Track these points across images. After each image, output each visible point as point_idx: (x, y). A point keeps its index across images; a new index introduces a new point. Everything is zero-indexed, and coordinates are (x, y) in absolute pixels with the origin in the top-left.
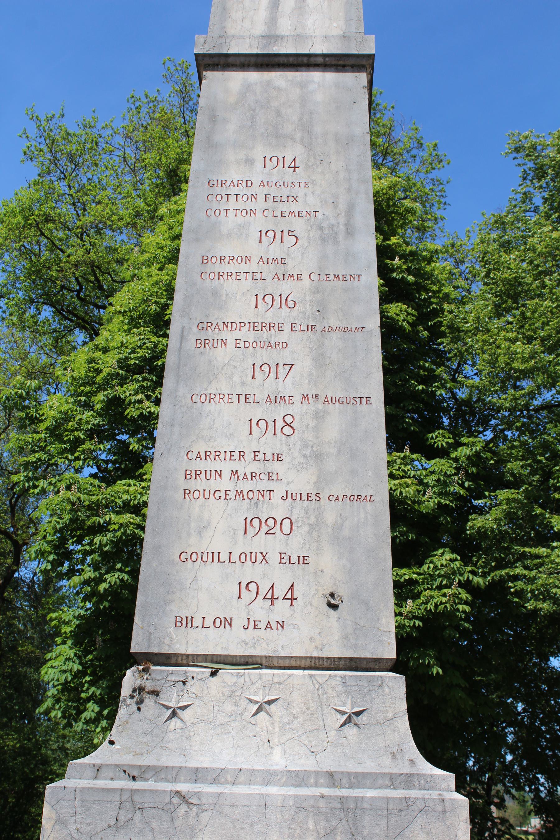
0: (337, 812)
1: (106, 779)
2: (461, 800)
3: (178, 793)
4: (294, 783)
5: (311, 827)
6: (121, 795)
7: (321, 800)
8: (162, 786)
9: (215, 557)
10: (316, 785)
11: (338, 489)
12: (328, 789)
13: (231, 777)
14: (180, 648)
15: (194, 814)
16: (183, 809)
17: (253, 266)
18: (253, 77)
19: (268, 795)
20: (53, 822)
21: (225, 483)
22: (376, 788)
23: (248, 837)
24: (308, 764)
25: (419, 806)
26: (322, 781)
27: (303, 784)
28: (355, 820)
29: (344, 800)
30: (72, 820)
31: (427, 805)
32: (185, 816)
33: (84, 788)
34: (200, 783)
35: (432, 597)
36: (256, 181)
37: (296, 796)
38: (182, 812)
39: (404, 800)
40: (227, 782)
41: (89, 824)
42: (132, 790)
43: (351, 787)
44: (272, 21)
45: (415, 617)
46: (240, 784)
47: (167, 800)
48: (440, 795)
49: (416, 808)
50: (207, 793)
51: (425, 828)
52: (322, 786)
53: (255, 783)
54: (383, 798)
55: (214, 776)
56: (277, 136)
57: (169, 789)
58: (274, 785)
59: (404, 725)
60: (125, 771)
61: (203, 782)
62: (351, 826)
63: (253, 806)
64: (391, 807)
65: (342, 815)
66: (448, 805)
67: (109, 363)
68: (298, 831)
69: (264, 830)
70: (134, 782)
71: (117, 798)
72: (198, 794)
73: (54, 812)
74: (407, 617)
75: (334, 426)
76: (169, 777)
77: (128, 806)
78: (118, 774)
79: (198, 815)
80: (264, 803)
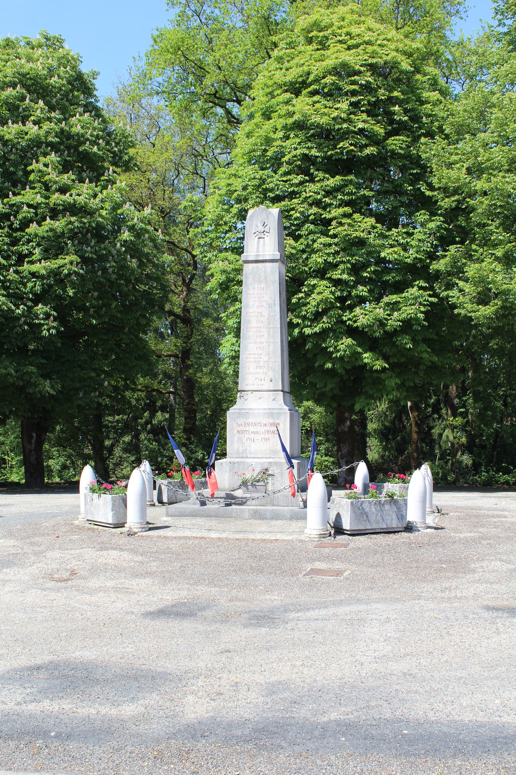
9: (251, 373)
11: (272, 360)
14: (246, 389)
17: (256, 314)
18: (254, 265)
21: (253, 360)
24: (267, 407)
35: (406, 310)
36: (256, 293)
44: (258, 249)
45: (399, 321)
59: (282, 400)
67: (238, 184)
74: (394, 321)
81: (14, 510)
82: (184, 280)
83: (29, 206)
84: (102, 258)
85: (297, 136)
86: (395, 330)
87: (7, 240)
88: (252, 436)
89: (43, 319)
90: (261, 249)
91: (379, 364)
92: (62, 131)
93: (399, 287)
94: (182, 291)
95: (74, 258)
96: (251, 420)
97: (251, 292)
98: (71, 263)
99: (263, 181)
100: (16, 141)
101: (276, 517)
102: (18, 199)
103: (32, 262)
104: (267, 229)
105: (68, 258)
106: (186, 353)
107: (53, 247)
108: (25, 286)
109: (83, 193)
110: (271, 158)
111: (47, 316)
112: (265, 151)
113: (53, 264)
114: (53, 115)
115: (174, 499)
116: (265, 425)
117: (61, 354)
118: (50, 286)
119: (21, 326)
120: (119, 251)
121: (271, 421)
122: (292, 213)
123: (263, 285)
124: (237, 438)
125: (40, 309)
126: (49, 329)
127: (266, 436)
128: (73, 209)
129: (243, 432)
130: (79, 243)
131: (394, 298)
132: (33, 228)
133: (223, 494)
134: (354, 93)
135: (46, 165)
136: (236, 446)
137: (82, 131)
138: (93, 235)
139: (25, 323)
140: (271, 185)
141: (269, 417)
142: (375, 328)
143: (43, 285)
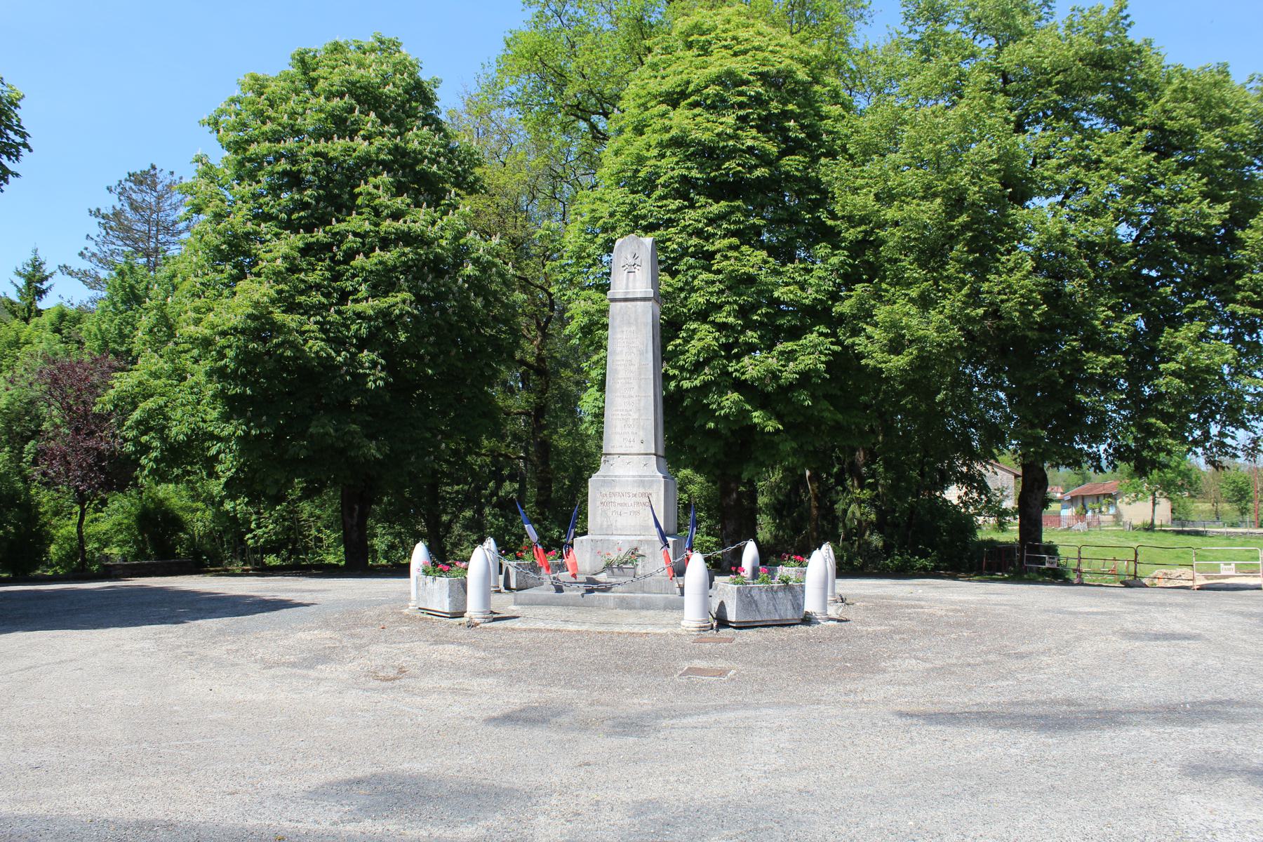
44: (627, 287)
56: (629, 324)
67: (604, 210)
75: (642, 404)
81: (331, 596)
82: (538, 324)
83: (356, 234)
84: (440, 297)
85: (674, 154)
86: (791, 383)
87: (328, 274)
88: (619, 509)
89: (369, 368)
90: (631, 285)
91: (1145, 271)
92: (396, 147)
93: (795, 334)
94: (536, 336)
95: (407, 295)
96: (617, 490)
97: (619, 336)
98: (404, 302)
99: (634, 207)
100: (342, 158)
101: (647, 606)
102: (342, 226)
103: (357, 301)
104: (638, 262)
105: (401, 296)
106: (538, 412)
107: (383, 282)
108: (348, 329)
109: (419, 219)
110: (644, 179)
111: (374, 364)
112: (637, 171)
113: (382, 303)
114: (386, 128)
115: (523, 585)
117: (393, 410)
118: (378, 329)
119: (342, 376)
120: (460, 288)
121: (642, 490)
122: (668, 244)
123: (633, 328)
125: (366, 356)
126: (376, 380)
127: (636, 508)
128: (407, 238)
130: (414, 278)
131: (790, 346)
132: (359, 260)
133: (581, 578)
134: (741, 106)
135: (377, 187)
136: (599, 520)
137: (419, 148)
138: (430, 268)
139: (347, 372)
140: (644, 212)
142: (767, 381)
143: (369, 327)
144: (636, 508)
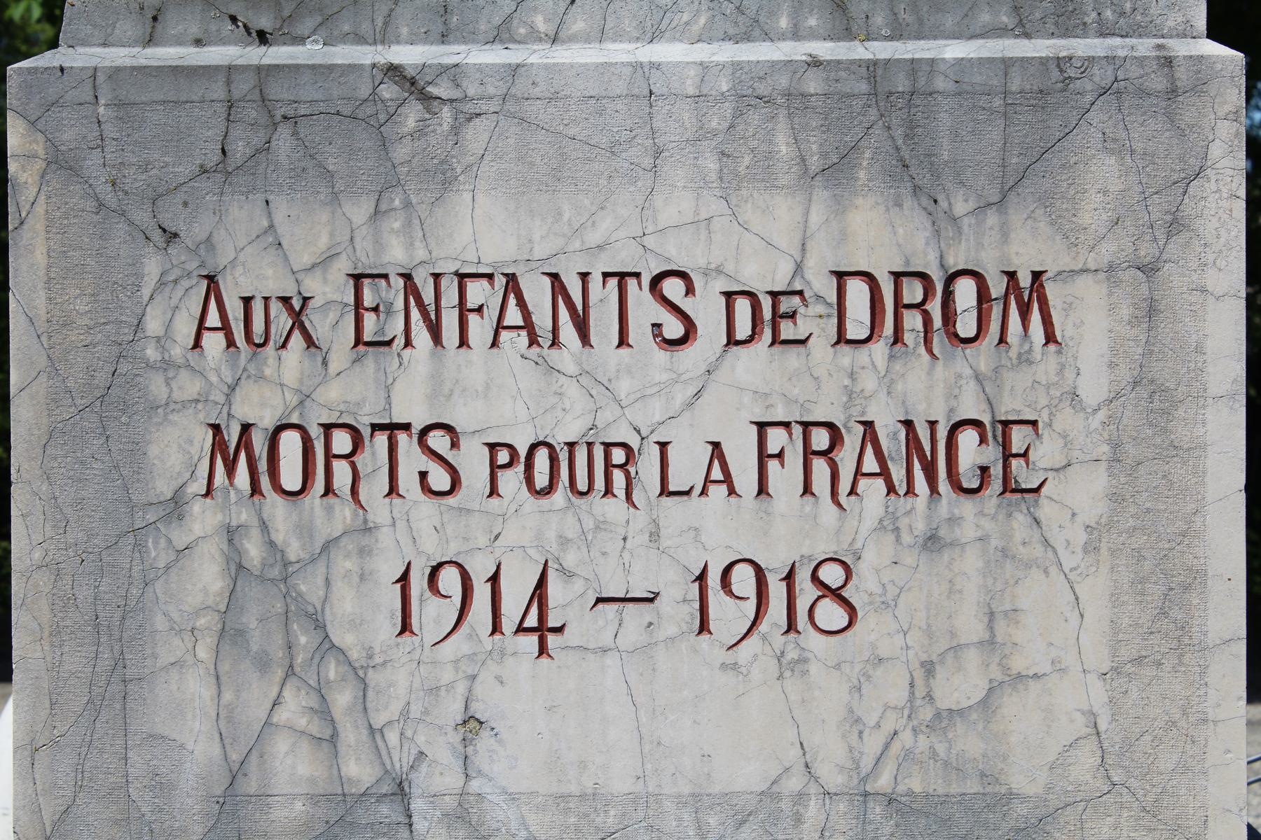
0: (858, 104)
1: (179, 42)
2: (1223, 59)
3: (393, 71)
4: (731, 32)
5: (783, 146)
6: (228, 83)
7: (812, 73)
8: (344, 54)
10: (796, 34)
12: (829, 44)
13: (547, 20)
15: (446, 127)
16: (412, 115)
19: (655, 66)
20: (40, 164)
22: (972, 37)
23: (603, 182)
25: (1097, 79)
26: (812, 22)
27: (757, 32)
28: (911, 125)
29: (880, 72)
30: (95, 158)
31: (1121, 75)
32: (420, 132)
33: (118, 69)
34: (457, 41)
37: (737, 66)
38: (411, 123)
39: (1052, 66)
40: (534, 36)
41: (145, 167)
42: (259, 69)
43: (897, 34)
46: (573, 39)
47: (364, 91)
48: (1159, 47)
49: (1089, 87)
50: (480, 68)
51: (1115, 140)
52: (813, 35)
53: (618, 37)
54: (991, 60)
55: (497, 20)
57: (368, 62)
58: (673, 39)
60: (234, 19)
61: (464, 41)
62: (900, 142)
63: (613, 99)
64: (1014, 86)
65: (873, 113)
66: (1183, 75)
68: (747, 160)
69: (647, 162)
70: (263, 48)
71: (218, 92)
72: (453, 72)
73: (40, 137)
76: (365, 28)
77: (254, 114)
78: (213, 28)
79: (456, 130)
80: (646, 88)
88: (516, 533)
96: (482, 228)
116: (768, 317)
121: (881, 234)
124: (207, 577)
127: (790, 527)
129: (334, 450)
141: (835, 171)
144: (790, 527)
